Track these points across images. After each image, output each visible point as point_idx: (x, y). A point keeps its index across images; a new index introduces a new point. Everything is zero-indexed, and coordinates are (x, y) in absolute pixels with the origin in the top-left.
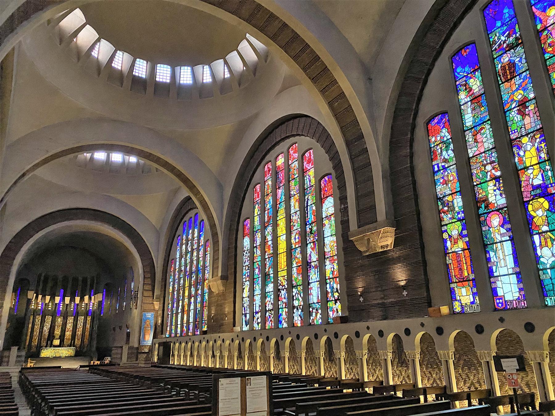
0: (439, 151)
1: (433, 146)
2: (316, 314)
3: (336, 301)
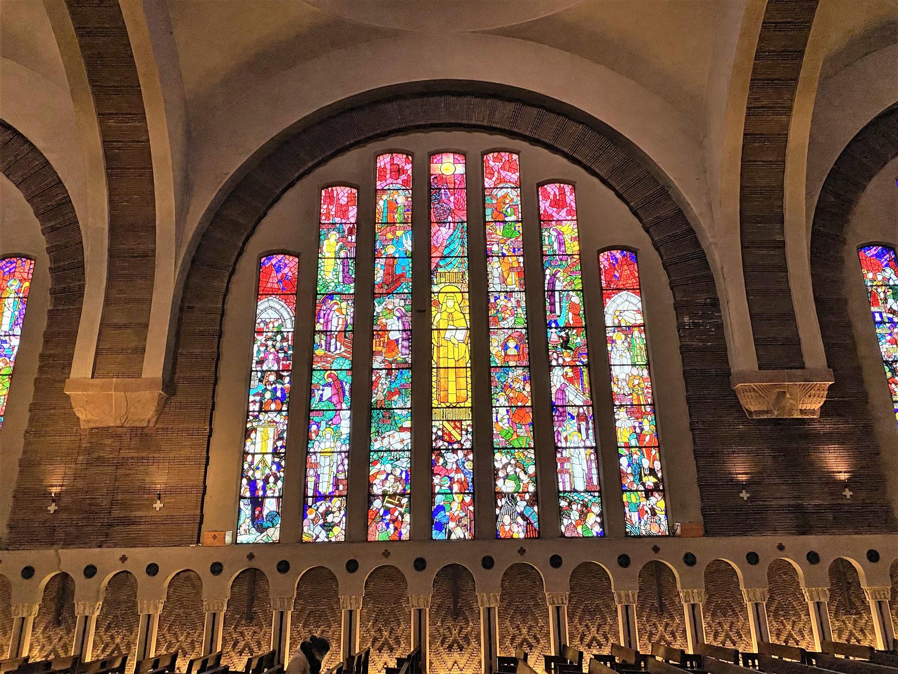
0: (882, 295)
1: (869, 284)
2: (583, 515)
3: (648, 493)
